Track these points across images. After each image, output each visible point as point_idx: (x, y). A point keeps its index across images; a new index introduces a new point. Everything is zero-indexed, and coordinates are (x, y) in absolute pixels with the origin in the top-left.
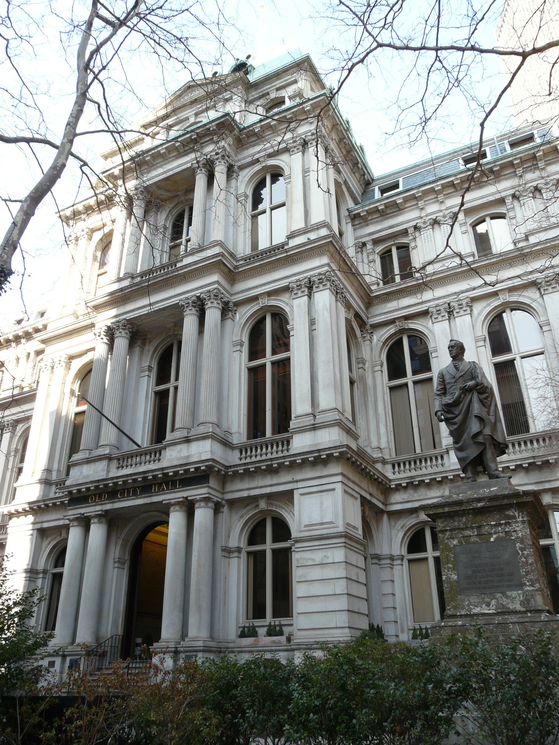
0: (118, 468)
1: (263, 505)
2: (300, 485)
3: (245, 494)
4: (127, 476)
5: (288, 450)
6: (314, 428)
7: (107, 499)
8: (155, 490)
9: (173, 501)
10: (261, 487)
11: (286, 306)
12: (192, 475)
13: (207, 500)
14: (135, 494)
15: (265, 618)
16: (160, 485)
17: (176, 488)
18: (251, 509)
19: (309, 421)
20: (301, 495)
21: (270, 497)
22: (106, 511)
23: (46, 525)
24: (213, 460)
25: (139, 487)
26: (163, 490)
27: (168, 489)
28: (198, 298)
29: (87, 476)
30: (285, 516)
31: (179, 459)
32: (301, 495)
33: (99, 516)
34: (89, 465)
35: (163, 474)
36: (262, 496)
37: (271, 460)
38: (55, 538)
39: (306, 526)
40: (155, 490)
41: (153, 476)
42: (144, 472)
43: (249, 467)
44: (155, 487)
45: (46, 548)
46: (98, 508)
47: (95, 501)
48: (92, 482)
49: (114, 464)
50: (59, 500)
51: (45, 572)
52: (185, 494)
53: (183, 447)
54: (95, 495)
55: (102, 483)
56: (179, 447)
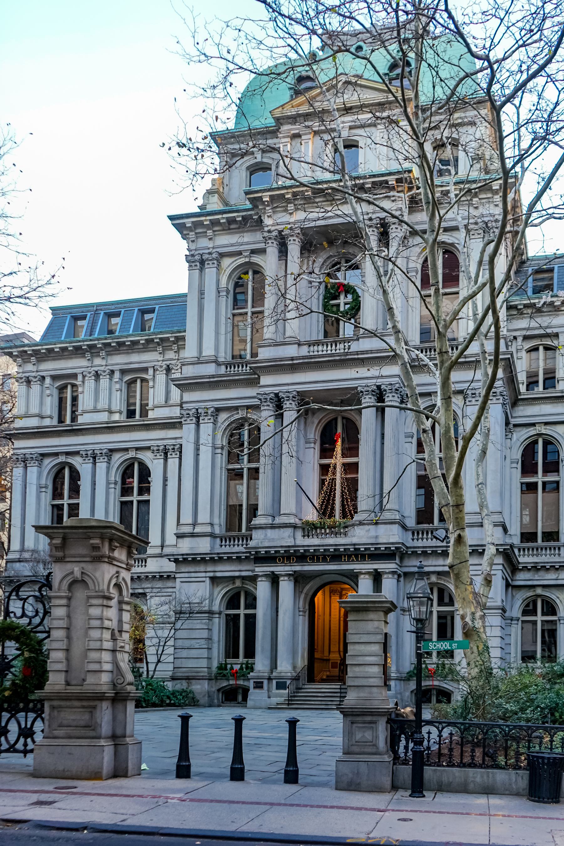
0: (304, 536)
8: (345, 560)
13: (394, 573)
14: (324, 560)
16: (349, 556)
17: (365, 560)
22: (295, 572)
23: (219, 574)
24: (403, 544)
25: (328, 556)
26: (353, 561)
27: (357, 560)
28: (379, 387)
35: (355, 549)
38: (227, 586)
40: (345, 560)
42: (336, 545)
44: (345, 557)
46: (287, 568)
47: (283, 562)
49: (299, 533)
51: (220, 613)
52: (376, 566)
53: (372, 527)
54: (283, 557)
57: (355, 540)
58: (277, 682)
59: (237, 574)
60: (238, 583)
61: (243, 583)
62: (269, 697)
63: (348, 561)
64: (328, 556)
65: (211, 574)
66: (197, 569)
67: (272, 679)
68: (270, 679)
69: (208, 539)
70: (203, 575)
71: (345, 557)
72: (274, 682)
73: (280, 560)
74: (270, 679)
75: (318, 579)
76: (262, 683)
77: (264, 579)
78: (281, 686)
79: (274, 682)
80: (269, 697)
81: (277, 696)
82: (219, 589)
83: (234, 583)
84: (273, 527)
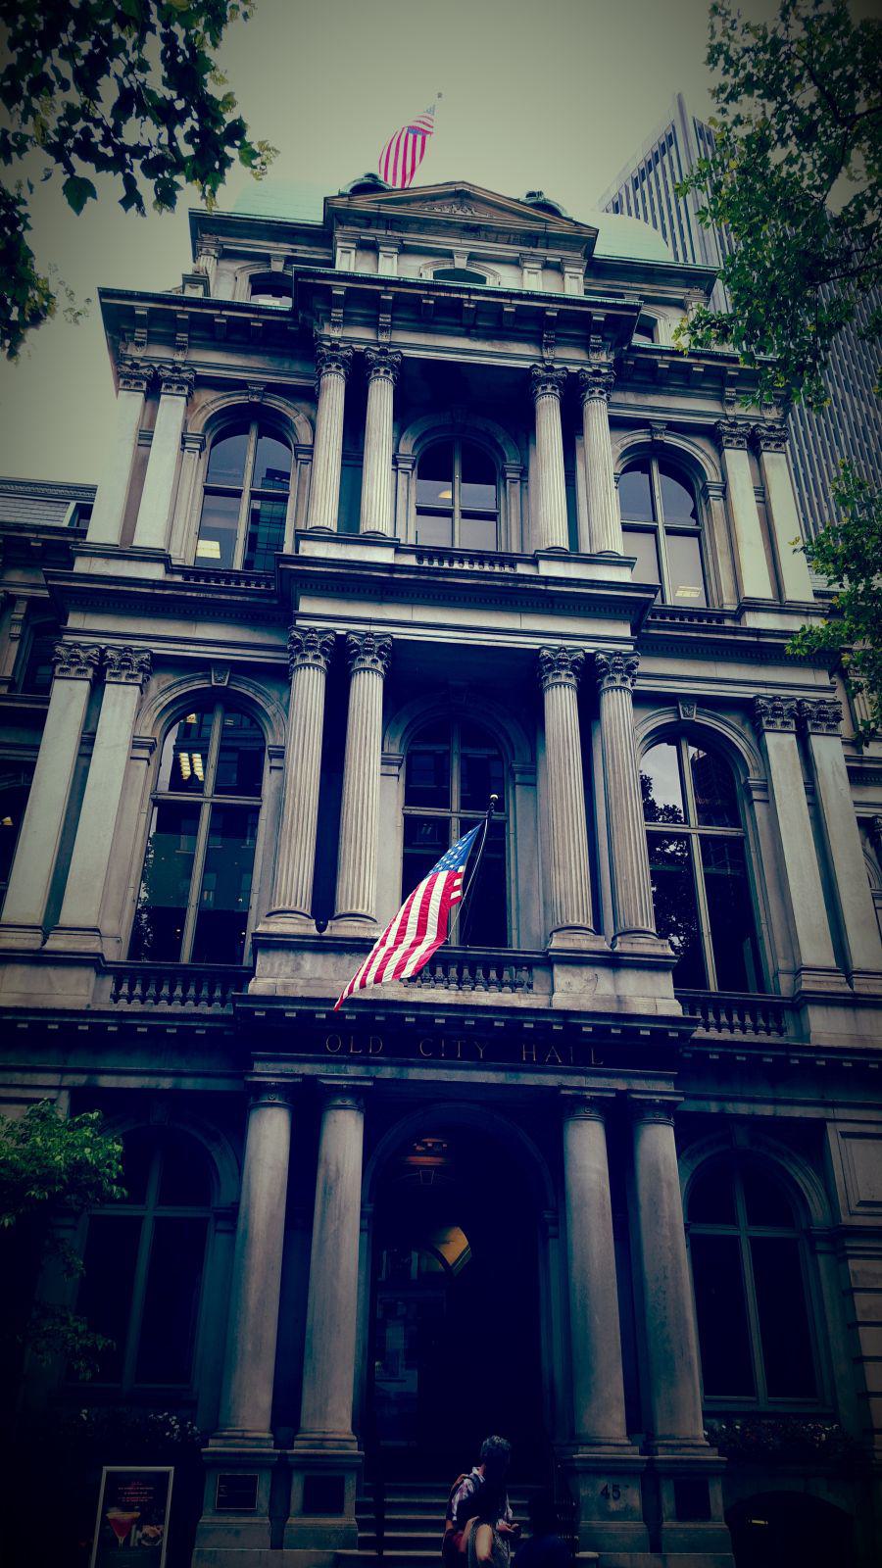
1: (741, 1139)
2: (841, 1113)
6: (40, 959)
8: (530, 1057)
19: (30, 941)
20: (845, 1135)
26: (553, 1061)
31: (604, 1000)
32: (845, 1135)
34: (320, 958)
39: (863, 1203)
40: (530, 1057)
41: (388, 1016)
46: (353, 1071)
52: (621, 1085)
55: (382, 1011)
56: (588, 973)
57: (560, 1001)
59: (166, 1083)
62: (277, 1544)
63: (539, 1062)
65: (81, 1080)
66: (36, 1061)
68: (282, 1470)
69: (88, 975)
70: (52, 1079)
71: (529, 1049)
74: (282, 1470)
76: (252, 1483)
78: (324, 1497)
80: (277, 1544)
81: (305, 1539)
84: (323, 946)
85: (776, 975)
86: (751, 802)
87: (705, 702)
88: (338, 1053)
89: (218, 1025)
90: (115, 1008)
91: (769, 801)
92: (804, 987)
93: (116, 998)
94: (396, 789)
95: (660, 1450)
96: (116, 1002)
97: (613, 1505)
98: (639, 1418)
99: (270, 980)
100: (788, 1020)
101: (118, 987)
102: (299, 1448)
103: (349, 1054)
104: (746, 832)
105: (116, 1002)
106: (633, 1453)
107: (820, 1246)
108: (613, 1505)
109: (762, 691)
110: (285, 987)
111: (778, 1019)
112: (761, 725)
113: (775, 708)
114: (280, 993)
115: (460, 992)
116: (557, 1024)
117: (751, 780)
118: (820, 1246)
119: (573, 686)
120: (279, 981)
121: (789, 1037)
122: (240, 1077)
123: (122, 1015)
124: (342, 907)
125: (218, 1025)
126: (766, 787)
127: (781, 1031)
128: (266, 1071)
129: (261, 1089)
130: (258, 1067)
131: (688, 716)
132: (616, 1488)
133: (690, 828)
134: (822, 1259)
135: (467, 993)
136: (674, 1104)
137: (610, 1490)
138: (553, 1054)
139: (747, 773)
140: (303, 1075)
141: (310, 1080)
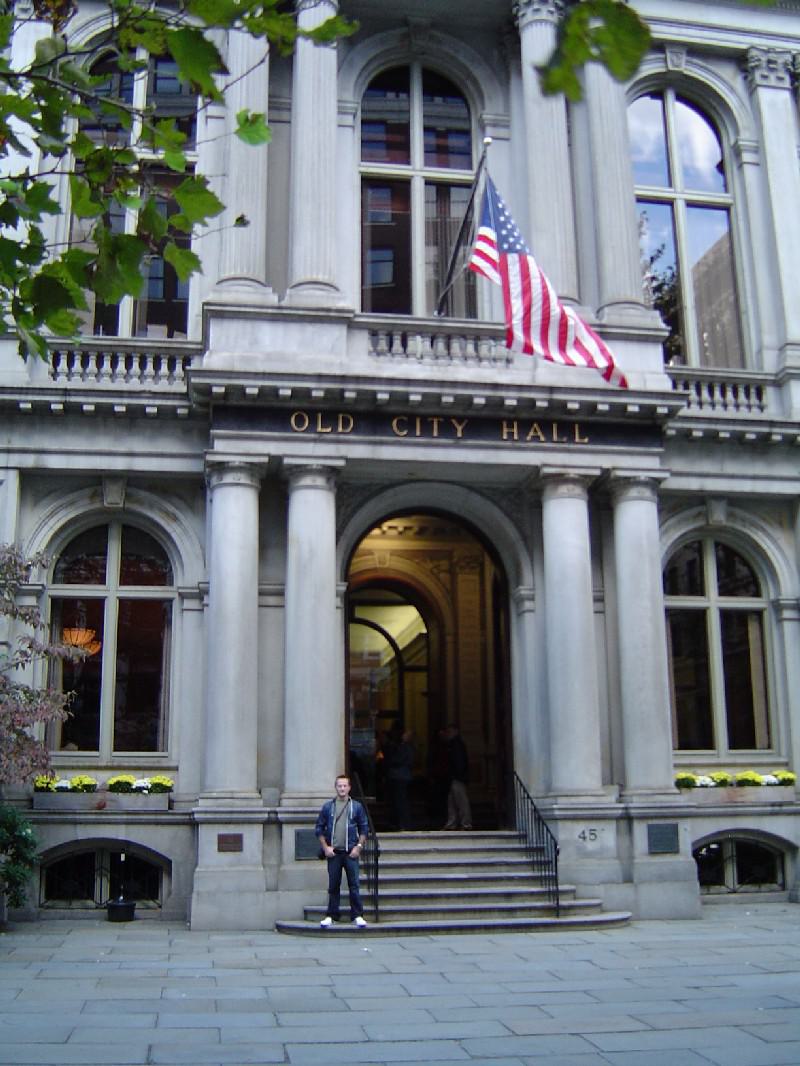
1: (719, 516)
3: (694, 484)
4: (442, 383)
5: (761, 408)
7: (355, 431)
8: (511, 434)
9: (573, 473)
10: (732, 477)
11: (727, 91)
12: (631, 421)
14: (447, 430)
15: (97, 749)
17: (572, 440)
18: (686, 519)
21: (734, 501)
26: (536, 438)
29: (282, 357)
30: (765, 547)
33: (330, 473)
35: (550, 401)
36: (719, 496)
37: (772, 424)
40: (511, 434)
42: (496, 386)
43: (718, 427)
44: (510, 426)
45: (38, 531)
47: (312, 428)
48: (320, 377)
50: (126, 401)
52: (606, 462)
58: (298, 834)
59: (119, 464)
60: (113, 498)
61: (128, 497)
63: (522, 438)
64: (460, 420)
65: (29, 461)
67: (279, 824)
71: (510, 426)
72: (289, 833)
73: (300, 421)
75: (390, 492)
77: (243, 478)
79: (289, 833)
82: (43, 512)
83: (98, 495)
85: (760, 352)
86: (740, 166)
87: (695, 51)
88: (303, 432)
89: (170, 403)
90: (53, 384)
91: (761, 165)
92: (789, 363)
93: (55, 375)
94: (352, 140)
95: (635, 799)
96: (55, 379)
97: (590, 846)
98: (615, 772)
99: (225, 354)
100: (769, 393)
101: (56, 363)
102: (288, 804)
103: (316, 432)
104: (734, 198)
105: (55, 379)
106: (610, 799)
107: (787, 614)
108: (590, 846)
109: (756, 41)
110: (243, 359)
111: (759, 395)
112: (752, 80)
113: (770, 62)
114: (239, 367)
115: (435, 368)
116: (543, 400)
117: (743, 141)
118: (787, 614)
119: (551, 23)
120: (237, 354)
121: (772, 412)
122: (201, 456)
123: (66, 392)
124: (301, 272)
125: (170, 403)
126: (759, 149)
127: (761, 408)
128: (231, 447)
129: (221, 468)
130: (219, 445)
131: (677, 66)
132: (592, 832)
133: (675, 192)
134: (788, 627)
135: (442, 368)
136: (658, 481)
137: (587, 834)
138: (535, 431)
139: (737, 132)
140: (268, 455)
141: (276, 460)
